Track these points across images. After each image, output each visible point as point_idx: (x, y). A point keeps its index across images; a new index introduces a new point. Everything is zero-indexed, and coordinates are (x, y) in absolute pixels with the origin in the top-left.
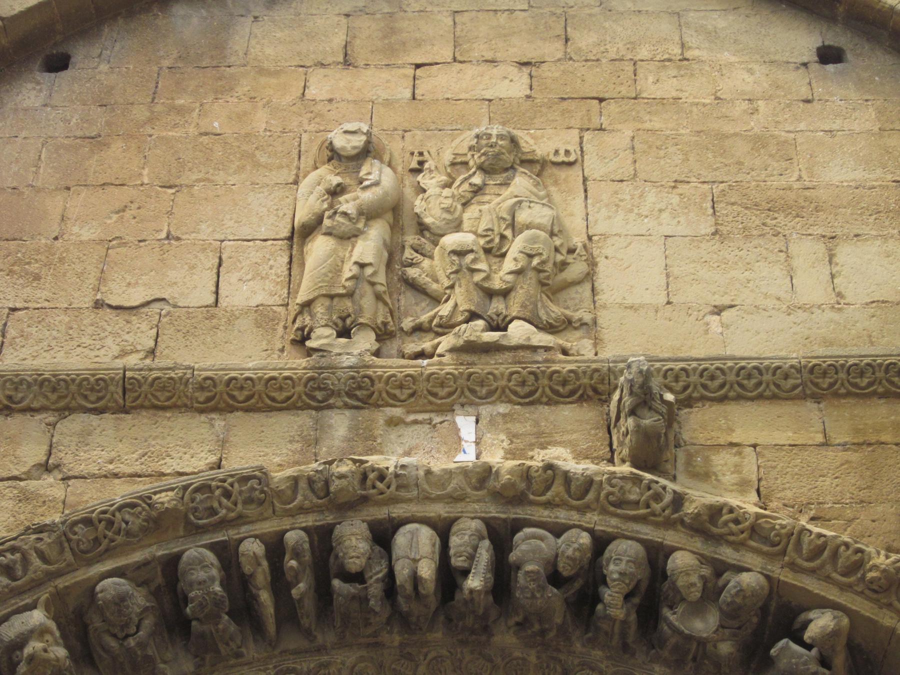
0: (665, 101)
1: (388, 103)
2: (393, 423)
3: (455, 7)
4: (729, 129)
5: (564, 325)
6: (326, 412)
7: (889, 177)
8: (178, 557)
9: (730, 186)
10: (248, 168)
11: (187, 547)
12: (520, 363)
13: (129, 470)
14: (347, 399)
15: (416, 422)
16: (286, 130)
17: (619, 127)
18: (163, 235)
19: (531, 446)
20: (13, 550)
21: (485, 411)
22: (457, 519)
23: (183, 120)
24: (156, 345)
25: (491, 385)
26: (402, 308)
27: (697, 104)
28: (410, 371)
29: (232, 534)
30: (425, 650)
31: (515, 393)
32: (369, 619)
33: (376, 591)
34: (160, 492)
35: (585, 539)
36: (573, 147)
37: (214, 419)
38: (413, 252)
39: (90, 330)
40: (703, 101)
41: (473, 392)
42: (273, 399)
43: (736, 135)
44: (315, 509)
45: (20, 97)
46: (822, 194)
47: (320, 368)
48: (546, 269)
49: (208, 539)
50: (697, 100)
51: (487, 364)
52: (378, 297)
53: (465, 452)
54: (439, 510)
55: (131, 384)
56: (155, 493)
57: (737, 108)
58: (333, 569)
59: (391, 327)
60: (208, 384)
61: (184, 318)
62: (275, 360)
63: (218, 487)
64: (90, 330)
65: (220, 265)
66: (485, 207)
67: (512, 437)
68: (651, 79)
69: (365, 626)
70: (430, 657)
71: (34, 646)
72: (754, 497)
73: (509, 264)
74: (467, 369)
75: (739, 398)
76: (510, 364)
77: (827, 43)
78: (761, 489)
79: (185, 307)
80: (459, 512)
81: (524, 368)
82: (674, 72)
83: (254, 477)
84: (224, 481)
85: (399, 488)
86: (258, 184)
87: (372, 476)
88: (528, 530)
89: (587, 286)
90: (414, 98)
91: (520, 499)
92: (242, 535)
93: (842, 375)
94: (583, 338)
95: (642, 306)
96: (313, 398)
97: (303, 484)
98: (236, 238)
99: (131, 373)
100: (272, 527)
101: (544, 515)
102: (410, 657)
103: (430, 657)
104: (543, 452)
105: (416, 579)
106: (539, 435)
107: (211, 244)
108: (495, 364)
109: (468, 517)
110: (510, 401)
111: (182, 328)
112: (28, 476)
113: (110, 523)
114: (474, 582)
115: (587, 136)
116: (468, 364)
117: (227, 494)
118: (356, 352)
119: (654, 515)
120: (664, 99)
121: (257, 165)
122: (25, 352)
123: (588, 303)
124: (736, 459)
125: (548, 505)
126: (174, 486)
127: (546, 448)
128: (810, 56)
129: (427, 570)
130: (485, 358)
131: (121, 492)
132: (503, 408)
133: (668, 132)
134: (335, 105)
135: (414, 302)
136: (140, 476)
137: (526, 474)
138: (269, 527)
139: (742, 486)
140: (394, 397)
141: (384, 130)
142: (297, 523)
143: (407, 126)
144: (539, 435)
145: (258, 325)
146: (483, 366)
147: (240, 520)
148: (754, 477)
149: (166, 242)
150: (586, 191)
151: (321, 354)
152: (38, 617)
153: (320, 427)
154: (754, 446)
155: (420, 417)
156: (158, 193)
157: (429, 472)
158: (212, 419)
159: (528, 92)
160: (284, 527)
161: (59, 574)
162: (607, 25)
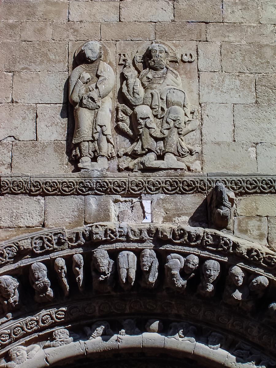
0: (235, 25)
1: (108, 24)
2: (116, 201)
4: (264, 41)
6: (87, 196)
9: (263, 75)
10: (45, 62)
11: (33, 262)
12: (170, 176)
13: (6, 225)
14: (96, 191)
15: (126, 201)
16: (62, 40)
17: (214, 39)
18: (10, 100)
19: (174, 216)
21: (155, 197)
22: (143, 249)
23: (13, 32)
24: (12, 161)
25: (158, 186)
26: (118, 143)
27: (250, 26)
28: (123, 179)
29: (52, 255)
31: (168, 190)
34: (21, 240)
35: (196, 260)
37: (40, 199)
38: (122, 114)
40: (253, 24)
42: (65, 191)
43: (267, 45)
47: (85, 177)
48: (181, 127)
50: (250, 24)
51: (156, 176)
52: (108, 141)
53: (146, 219)
55: (3, 184)
56: (19, 241)
57: (268, 30)
59: (115, 155)
60: (36, 185)
61: (22, 147)
63: (45, 238)
65: (37, 117)
67: (166, 210)
68: (230, 10)
72: (265, 242)
74: (147, 179)
75: (262, 193)
76: (165, 176)
78: (269, 238)
79: (23, 141)
81: (171, 179)
82: (240, 7)
83: (60, 233)
84: (47, 235)
85: (120, 236)
86: (50, 71)
87: (109, 232)
88: (173, 255)
89: (198, 132)
90: (120, 21)
92: (55, 257)
94: (196, 160)
95: (223, 143)
96: (82, 190)
97: (81, 236)
98: (43, 102)
99: (3, 178)
100: (68, 253)
104: (179, 219)
105: (128, 277)
106: (177, 209)
107: (31, 105)
108: (159, 177)
110: (166, 193)
111: (22, 152)
115: (200, 45)
116: (147, 176)
117: (49, 241)
118: (100, 169)
120: (235, 23)
121: (49, 60)
123: (198, 141)
124: (259, 223)
126: (27, 238)
127: (180, 217)
129: (133, 275)
130: (155, 174)
132: (162, 196)
133: (236, 43)
134: (83, 24)
135: (123, 140)
136: (10, 228)
139: (261, 236)
140: (116, 190)
141: (107, 40)
142: (78, 251)
143: (116, 38)
144: (177, 209)
145: (56, 151)
146: (153, 177)
147: (54, 250)
148: (266, 233)
149: (11, 104)
150: (199, 77)
151: (84, 170)
153: (85, 203)
154: (267, 216)
155: (127, 199)
156: (5, 75)
158: (39, 199)
159: (172, 18)
160: (73, 253)
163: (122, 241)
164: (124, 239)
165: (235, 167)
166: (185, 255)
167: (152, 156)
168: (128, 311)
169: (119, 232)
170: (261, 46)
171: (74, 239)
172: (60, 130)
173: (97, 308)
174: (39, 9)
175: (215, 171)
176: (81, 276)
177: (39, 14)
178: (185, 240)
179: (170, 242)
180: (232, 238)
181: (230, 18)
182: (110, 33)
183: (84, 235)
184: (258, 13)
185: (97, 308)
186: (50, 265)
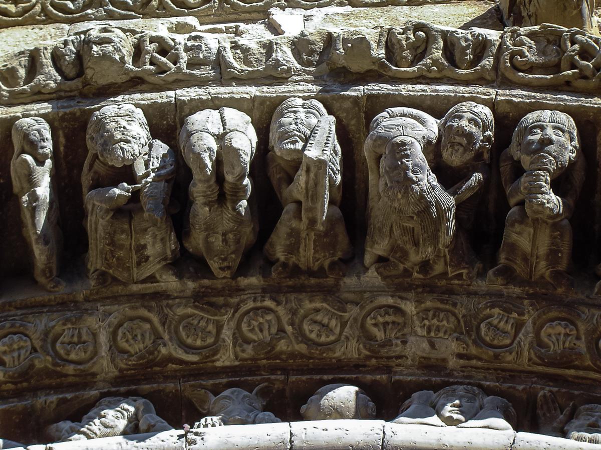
14: (111, 7)
30: (234, 300)
32: (144, 247)
33: (156, 191)
35: (485, 112)
44: (63, 94)
69: (139, 264)
70: (244, 308)
80: (283, 92)
85: (190, 65)
87: (151, 47)
103: (244, 308)
109: (299, 97)
119: (585, 77)
155: (222, 26)
163: (202, 83)
164: (206, 72)
166: (437, 107)
168: (225, 359)
169: (187, 49)
171: (22, 72)
173: (103, 338)
176: (43, 190)
178: (435, 62)
179: (377, 74)
183: (57, 57)
185: (103, 338)
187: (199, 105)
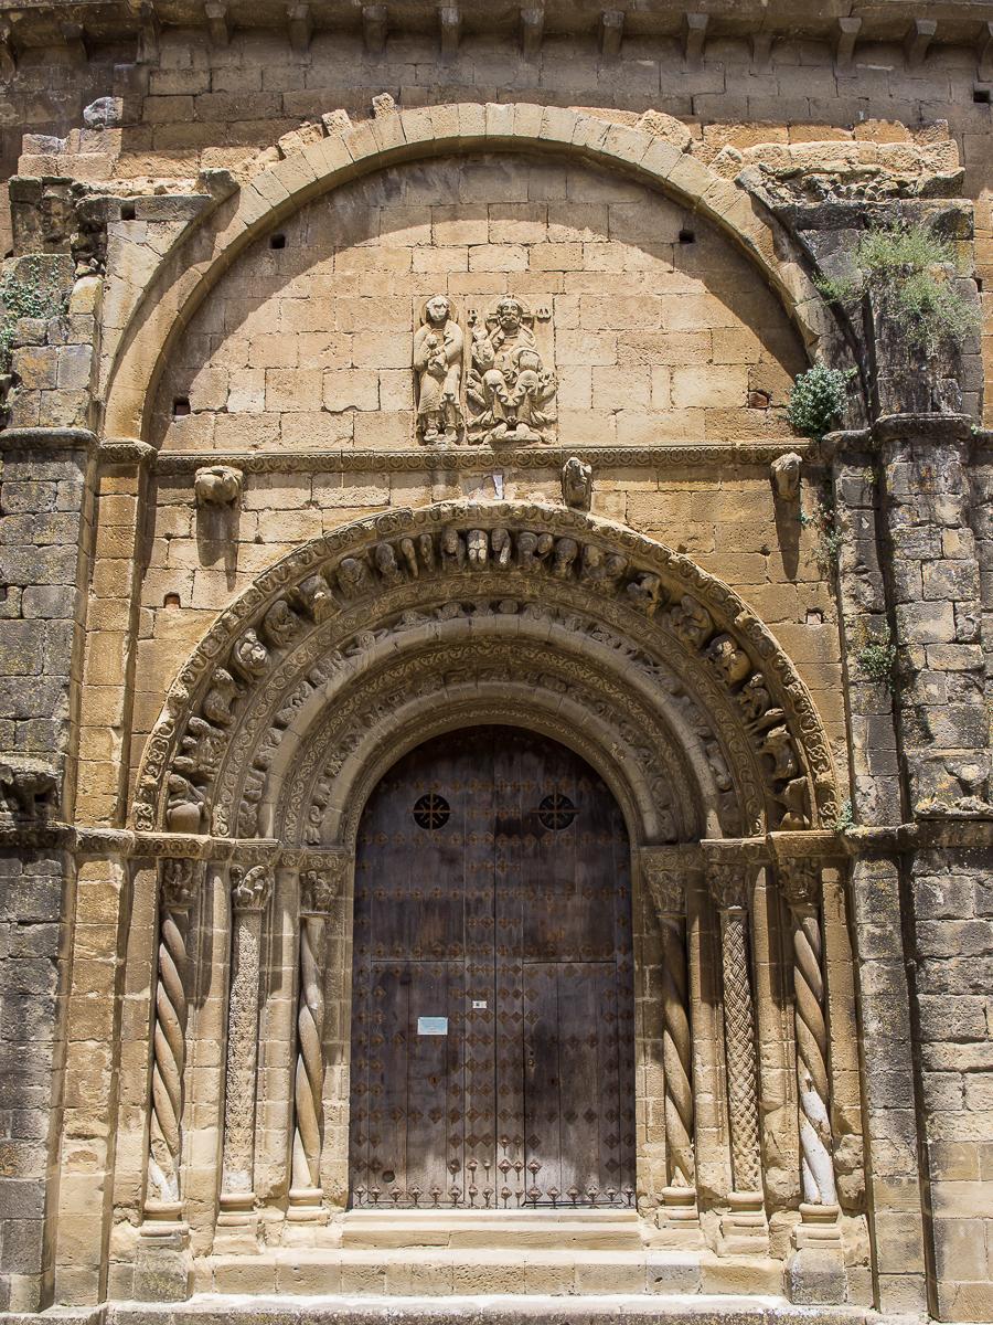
3: (489, 201)
4: (628, 293)
5: (546, 423)
7: (707, 326)
8: (376, 548)
20: (304, 552)
21: (507, 472)
28: (473, 453)
35: (550, 539)
36: (549, 308)
39: (321, 425)
41: (502, 464)
43: (632, 297)
45: (262, 269)
46: (670, 337)
49: (387, 540)
54: (486, 525)
58: (442, 548)
62: (407, 447)
64: (321, 425)
66: (505, 354)
71: (319, 594)
72: (624, 520)
73: (517, 393)
75: (621, 466)
77: (687, 228)
91: (521, 521)
93: (668, 456)
97: (428, 515)
101: (532, 527)
102: (476, 581)
105: (478, 558)
112: (303, 508)
113: (345, 537)
114: (503, 560)
121: (392, 319)
122: (292, 439)
123: (554, 409)
125: (534, 523)
128: (674, 238)
129: (483, 554)
131: (348, 525)
132: (515, 470)
137: (524, 509)
138: (413, 534)
147: (402, 531)
152: (318, 580)
157: (482, 508)
161: (325, 559)
162: (569, 215)
165: (593, 437)
167: (503, 426)
170: (626, 298)
172: (405, 398)
174: (380, 258)
175: (570, 443)
177: (379, 264)
180: (589, 516)
181: (591, 265)
182: (458, 286)
184: (622, 258)
186: (397, 546)
187: (472, 529)
